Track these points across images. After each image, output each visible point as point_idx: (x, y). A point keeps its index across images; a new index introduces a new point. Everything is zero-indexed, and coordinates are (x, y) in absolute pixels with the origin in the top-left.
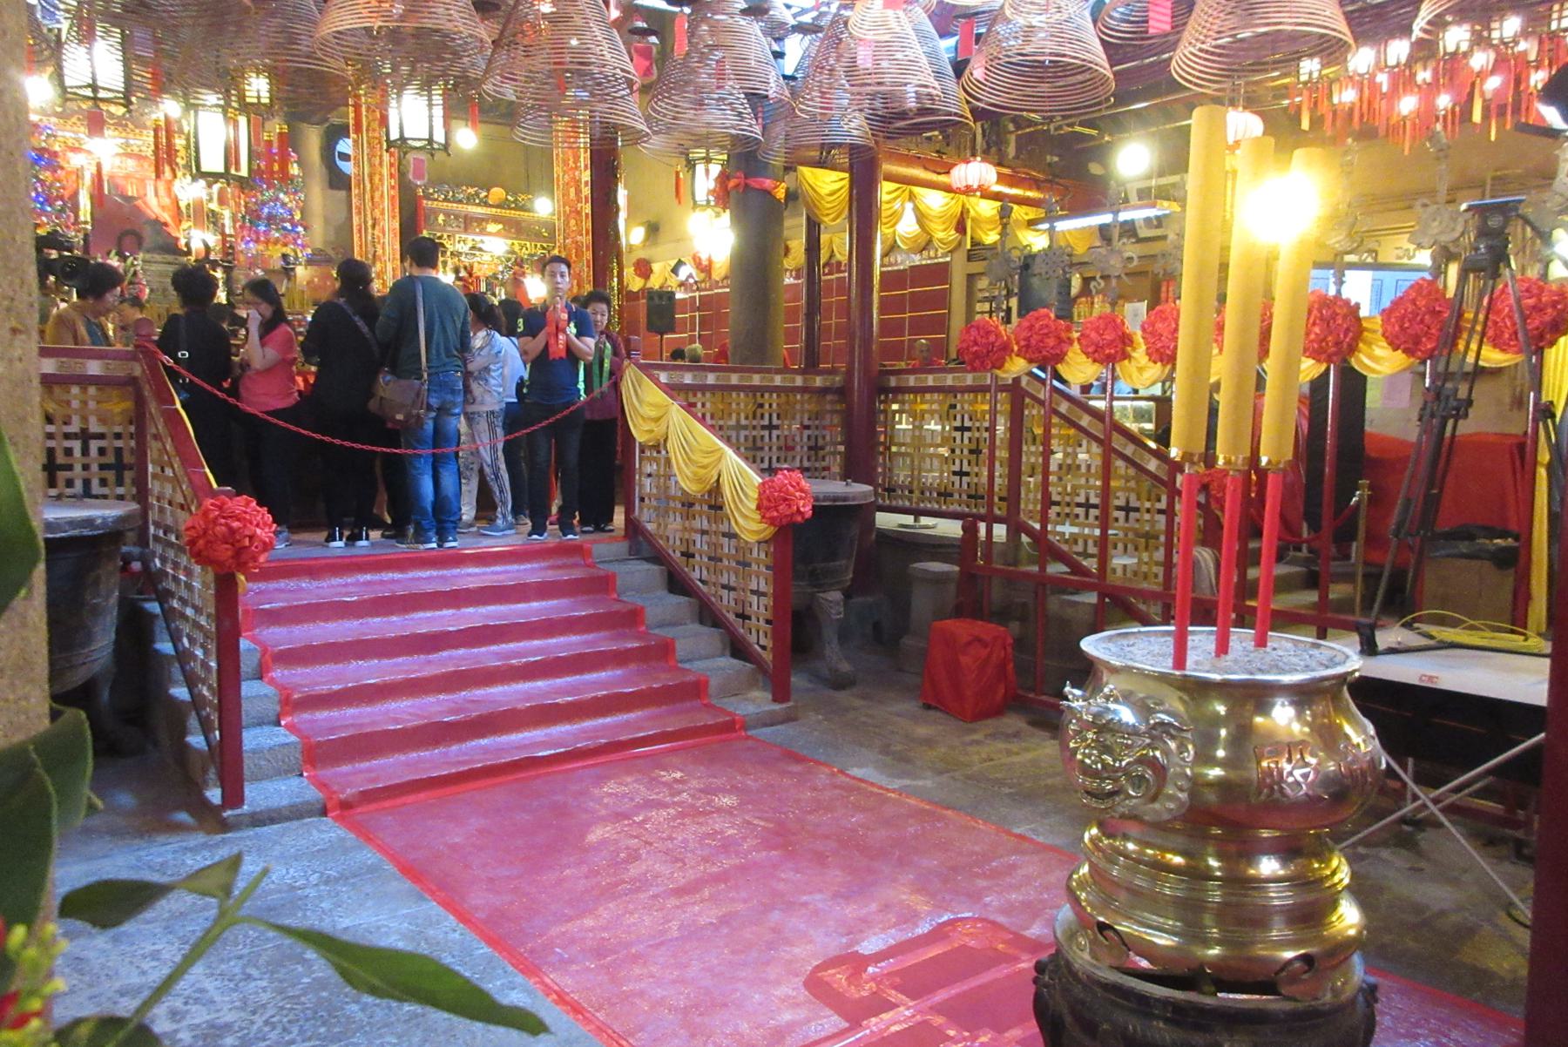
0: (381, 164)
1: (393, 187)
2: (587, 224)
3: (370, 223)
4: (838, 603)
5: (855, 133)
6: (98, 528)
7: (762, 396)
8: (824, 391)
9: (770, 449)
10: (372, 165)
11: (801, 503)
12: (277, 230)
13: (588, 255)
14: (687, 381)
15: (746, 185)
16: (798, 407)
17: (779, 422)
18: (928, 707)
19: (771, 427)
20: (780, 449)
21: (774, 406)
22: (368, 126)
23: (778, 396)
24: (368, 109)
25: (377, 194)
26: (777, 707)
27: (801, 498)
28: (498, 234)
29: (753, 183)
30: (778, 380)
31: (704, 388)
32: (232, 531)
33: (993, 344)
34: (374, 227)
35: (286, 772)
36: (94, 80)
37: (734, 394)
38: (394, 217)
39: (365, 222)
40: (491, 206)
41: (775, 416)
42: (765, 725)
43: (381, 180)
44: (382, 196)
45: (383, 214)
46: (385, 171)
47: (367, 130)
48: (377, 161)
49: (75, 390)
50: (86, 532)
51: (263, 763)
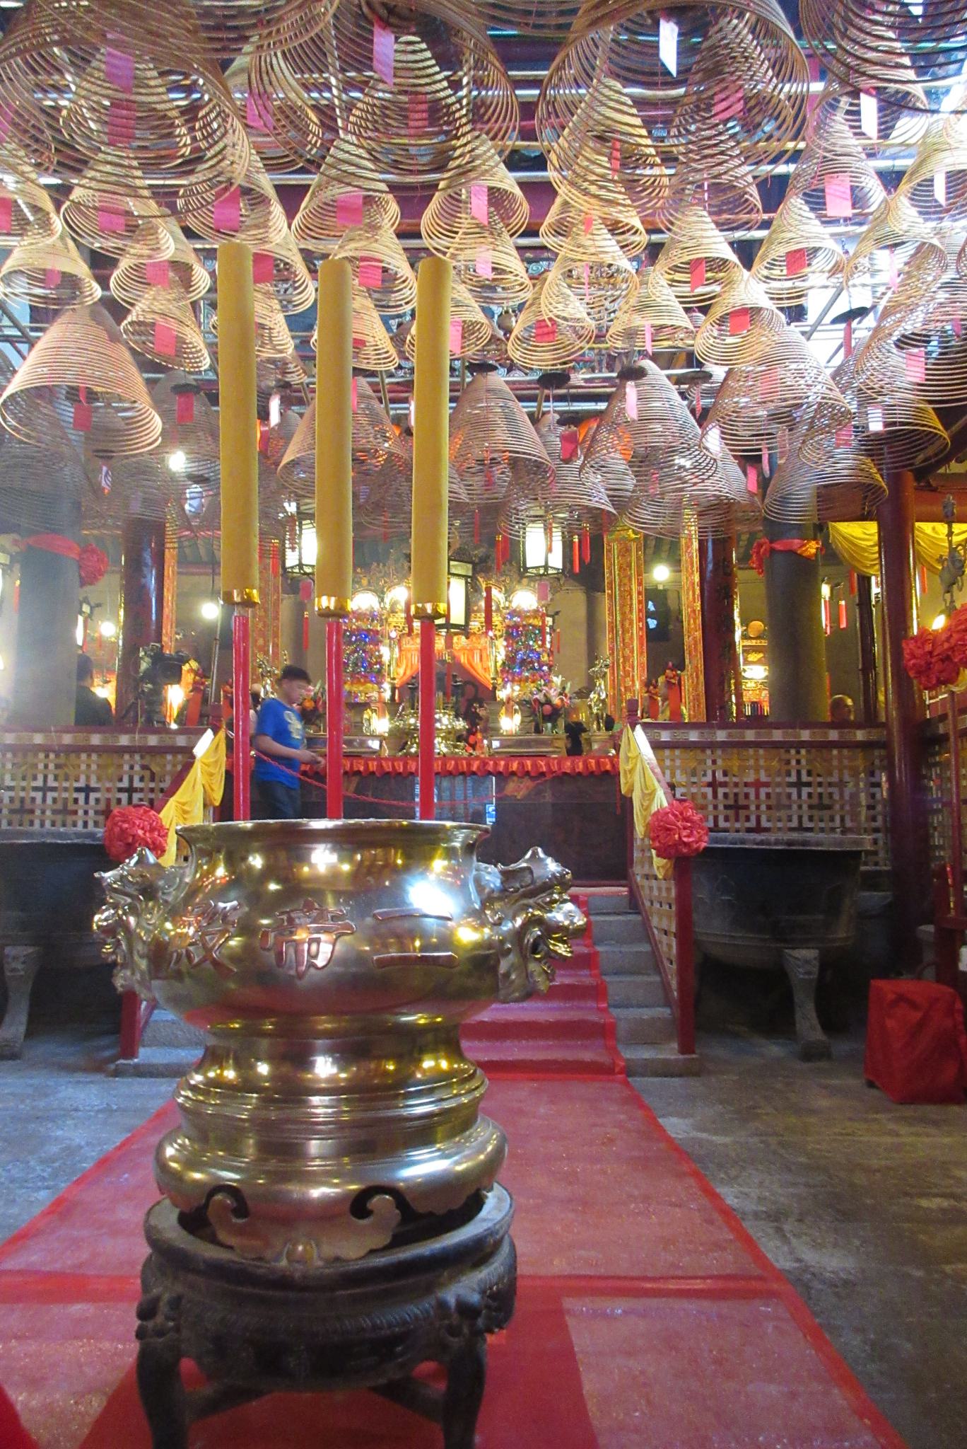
0: (631, 611)
1: (641, 629)
2: (699, 621)
3: (621, 660)
4: (807, 962)
5: (845, 472)
6: (98, 839)
7: (798, 752)
8: (867, 746)
9: (800, 807)
10: (623, 614)
11: (685, 833)
12: (528, 670)
13: (700, 648)
14: (692, 739)
15: (772, 550)
16: (835, 763)
17: (810, 779)
18: (871, 1084)
19: (799, 784)
20: (811, 807)
21: (803, 762)
22: (621, 581)
23: (808, 752)
24: (620, 568)
25: (628, 636)
26: (681, 1057)
27: (685, 828)
28: (759, 662)
29: (778, 546)
30: (805, 735)
31: (713, 746)
32: (123, 831)
33: (930, 653)
34: (624, 662)
35: (197, 1044)
36: (300, 560)
37: (751, 751)
38: (642, 653)
39: (618, 660)
40: (751, 638)
41: (804, 773)
42: (656, 1074)
43: (631, 624)
44: (631, 638)
45: (632, 652)
46: (634, 616)
47: (620, 586)
48: (627, 610)
49: (169, 757)
50: (88, 841)
51: (179, 1033)
